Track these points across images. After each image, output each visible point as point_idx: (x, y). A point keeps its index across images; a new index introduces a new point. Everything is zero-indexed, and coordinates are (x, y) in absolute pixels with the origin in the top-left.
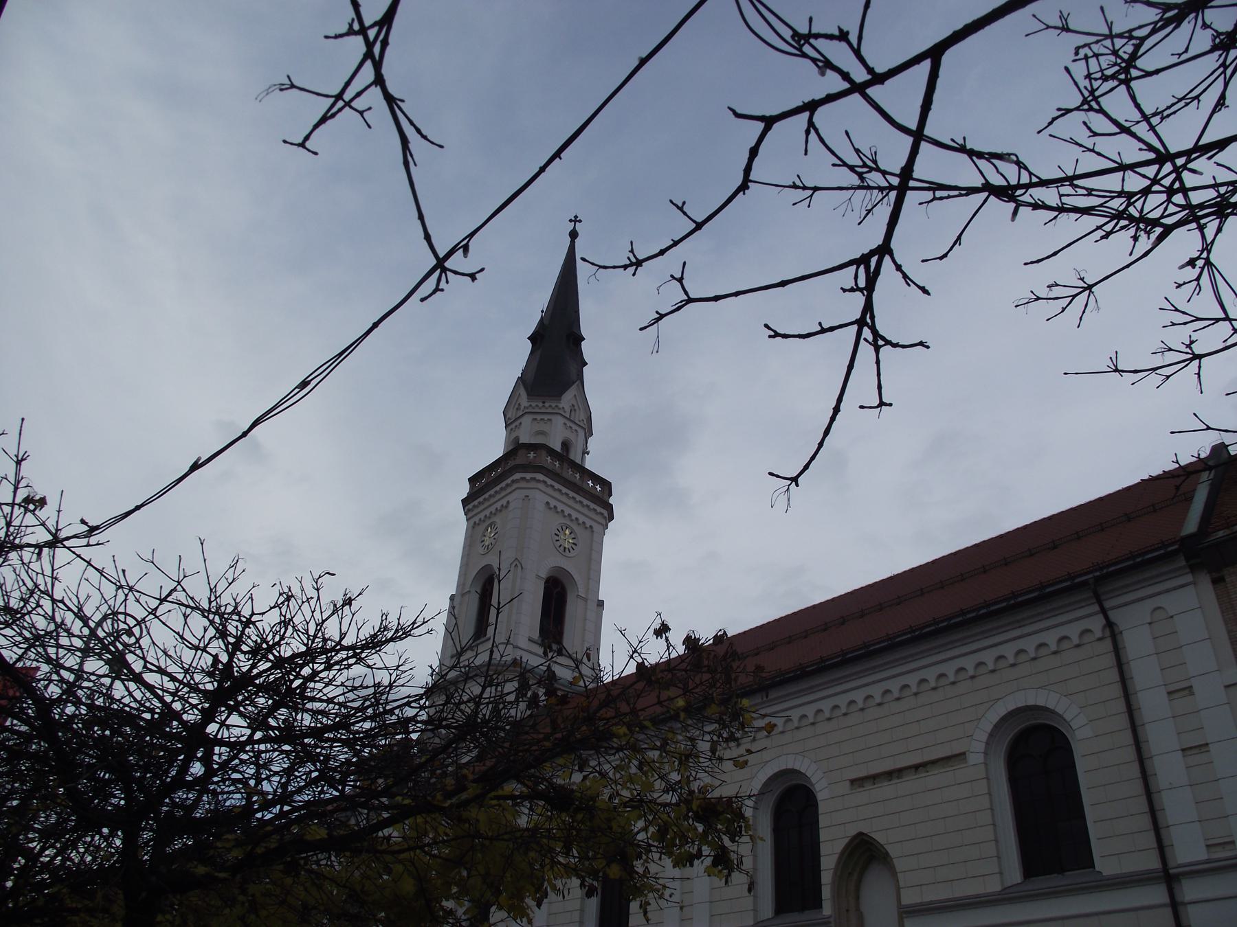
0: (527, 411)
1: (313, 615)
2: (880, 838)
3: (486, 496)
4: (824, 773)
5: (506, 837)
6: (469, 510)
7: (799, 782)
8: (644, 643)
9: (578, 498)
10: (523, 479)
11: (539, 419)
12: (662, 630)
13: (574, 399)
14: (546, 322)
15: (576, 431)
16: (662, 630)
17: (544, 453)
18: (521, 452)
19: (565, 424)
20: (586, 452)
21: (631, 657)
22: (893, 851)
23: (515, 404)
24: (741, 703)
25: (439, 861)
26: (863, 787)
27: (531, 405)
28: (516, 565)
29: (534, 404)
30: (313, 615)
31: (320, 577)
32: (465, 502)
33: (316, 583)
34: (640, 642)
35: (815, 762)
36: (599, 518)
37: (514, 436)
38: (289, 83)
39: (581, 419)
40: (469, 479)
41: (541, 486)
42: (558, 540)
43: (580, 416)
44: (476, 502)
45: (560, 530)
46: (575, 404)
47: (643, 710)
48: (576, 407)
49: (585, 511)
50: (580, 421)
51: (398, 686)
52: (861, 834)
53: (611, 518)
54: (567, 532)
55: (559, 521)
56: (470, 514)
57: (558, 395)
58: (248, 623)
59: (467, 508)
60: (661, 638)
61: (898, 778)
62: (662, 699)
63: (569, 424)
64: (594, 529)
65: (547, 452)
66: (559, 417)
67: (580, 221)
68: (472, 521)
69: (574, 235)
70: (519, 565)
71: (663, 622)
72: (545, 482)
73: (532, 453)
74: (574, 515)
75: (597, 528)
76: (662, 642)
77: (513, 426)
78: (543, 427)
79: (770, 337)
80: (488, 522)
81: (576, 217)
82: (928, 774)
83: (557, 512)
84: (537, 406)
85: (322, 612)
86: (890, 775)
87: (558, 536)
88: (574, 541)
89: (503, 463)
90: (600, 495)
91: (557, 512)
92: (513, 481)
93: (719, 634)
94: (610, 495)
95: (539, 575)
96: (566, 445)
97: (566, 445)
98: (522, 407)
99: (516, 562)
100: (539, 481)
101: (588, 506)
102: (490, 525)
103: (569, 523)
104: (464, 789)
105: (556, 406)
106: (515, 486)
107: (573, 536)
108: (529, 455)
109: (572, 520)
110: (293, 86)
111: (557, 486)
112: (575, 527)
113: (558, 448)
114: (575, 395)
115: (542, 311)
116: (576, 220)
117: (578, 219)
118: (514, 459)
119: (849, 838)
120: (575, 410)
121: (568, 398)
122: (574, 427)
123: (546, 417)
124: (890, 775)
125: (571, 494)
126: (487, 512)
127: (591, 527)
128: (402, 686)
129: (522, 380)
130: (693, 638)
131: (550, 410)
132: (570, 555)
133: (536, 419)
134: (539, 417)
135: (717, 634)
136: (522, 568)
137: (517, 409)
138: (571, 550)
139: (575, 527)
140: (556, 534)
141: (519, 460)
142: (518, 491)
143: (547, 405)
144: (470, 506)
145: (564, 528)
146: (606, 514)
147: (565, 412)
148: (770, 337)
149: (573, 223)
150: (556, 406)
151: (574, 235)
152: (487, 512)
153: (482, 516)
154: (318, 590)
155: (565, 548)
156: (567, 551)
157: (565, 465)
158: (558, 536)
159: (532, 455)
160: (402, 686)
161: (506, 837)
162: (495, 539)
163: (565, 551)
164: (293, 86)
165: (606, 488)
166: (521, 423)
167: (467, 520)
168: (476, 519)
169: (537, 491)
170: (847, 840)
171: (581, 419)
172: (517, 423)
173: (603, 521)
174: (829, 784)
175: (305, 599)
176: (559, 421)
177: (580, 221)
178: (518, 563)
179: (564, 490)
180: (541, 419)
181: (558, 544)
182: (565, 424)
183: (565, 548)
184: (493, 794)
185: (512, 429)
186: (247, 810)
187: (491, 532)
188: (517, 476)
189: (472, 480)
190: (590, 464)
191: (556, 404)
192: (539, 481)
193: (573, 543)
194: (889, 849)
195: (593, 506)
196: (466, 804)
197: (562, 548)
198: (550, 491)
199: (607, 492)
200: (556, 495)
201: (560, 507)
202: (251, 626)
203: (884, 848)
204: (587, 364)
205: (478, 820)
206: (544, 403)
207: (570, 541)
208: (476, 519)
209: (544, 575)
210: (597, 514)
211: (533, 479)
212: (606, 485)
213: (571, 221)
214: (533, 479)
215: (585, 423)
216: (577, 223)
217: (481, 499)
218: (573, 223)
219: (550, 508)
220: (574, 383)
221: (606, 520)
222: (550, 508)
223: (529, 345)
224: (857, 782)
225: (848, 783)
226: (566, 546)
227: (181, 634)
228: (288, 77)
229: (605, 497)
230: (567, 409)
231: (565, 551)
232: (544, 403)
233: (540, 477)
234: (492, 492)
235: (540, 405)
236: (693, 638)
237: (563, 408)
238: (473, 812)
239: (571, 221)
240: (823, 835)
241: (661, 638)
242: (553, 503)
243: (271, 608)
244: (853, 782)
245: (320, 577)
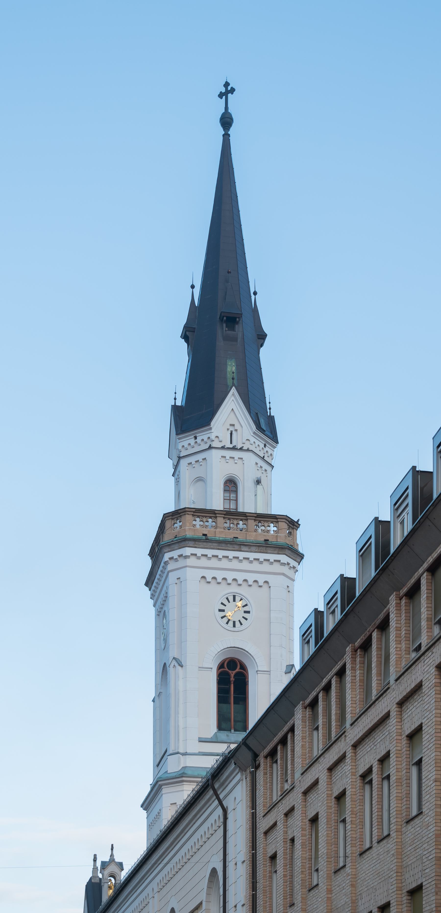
9: (241, 555)
13: (232, 413)
28: (174, 666)
36: (276, 568)
39: (244, 441)
41: (191, 561)
48: (237, 426)
74: (240, 577)
81: (227, 84)
83: (219, 583)
99: (174, 662)
103: (234, 589)
112: (243, 591)
114: (232, 409)
120: (236, 430)
122: (236, 454)
123: (200, 457)
125: (231, 554)
138: (243, 621)
139: (243, 591)
143: (199, 440)
146: (284, 558)
150: (209, 438)
155: (234, 622)
163: (234, 626)
165: (283, 525)
171: (244, 441)
177: (233, 90)
191: (208, 436)
198: (204, 562)
201: (219, 575)
215: (252, 440)
216: (230, 95)
231: (234, 626)
233: (188, 551)
235: (192, 441)
237: (217, 437)
242: (209, 576)
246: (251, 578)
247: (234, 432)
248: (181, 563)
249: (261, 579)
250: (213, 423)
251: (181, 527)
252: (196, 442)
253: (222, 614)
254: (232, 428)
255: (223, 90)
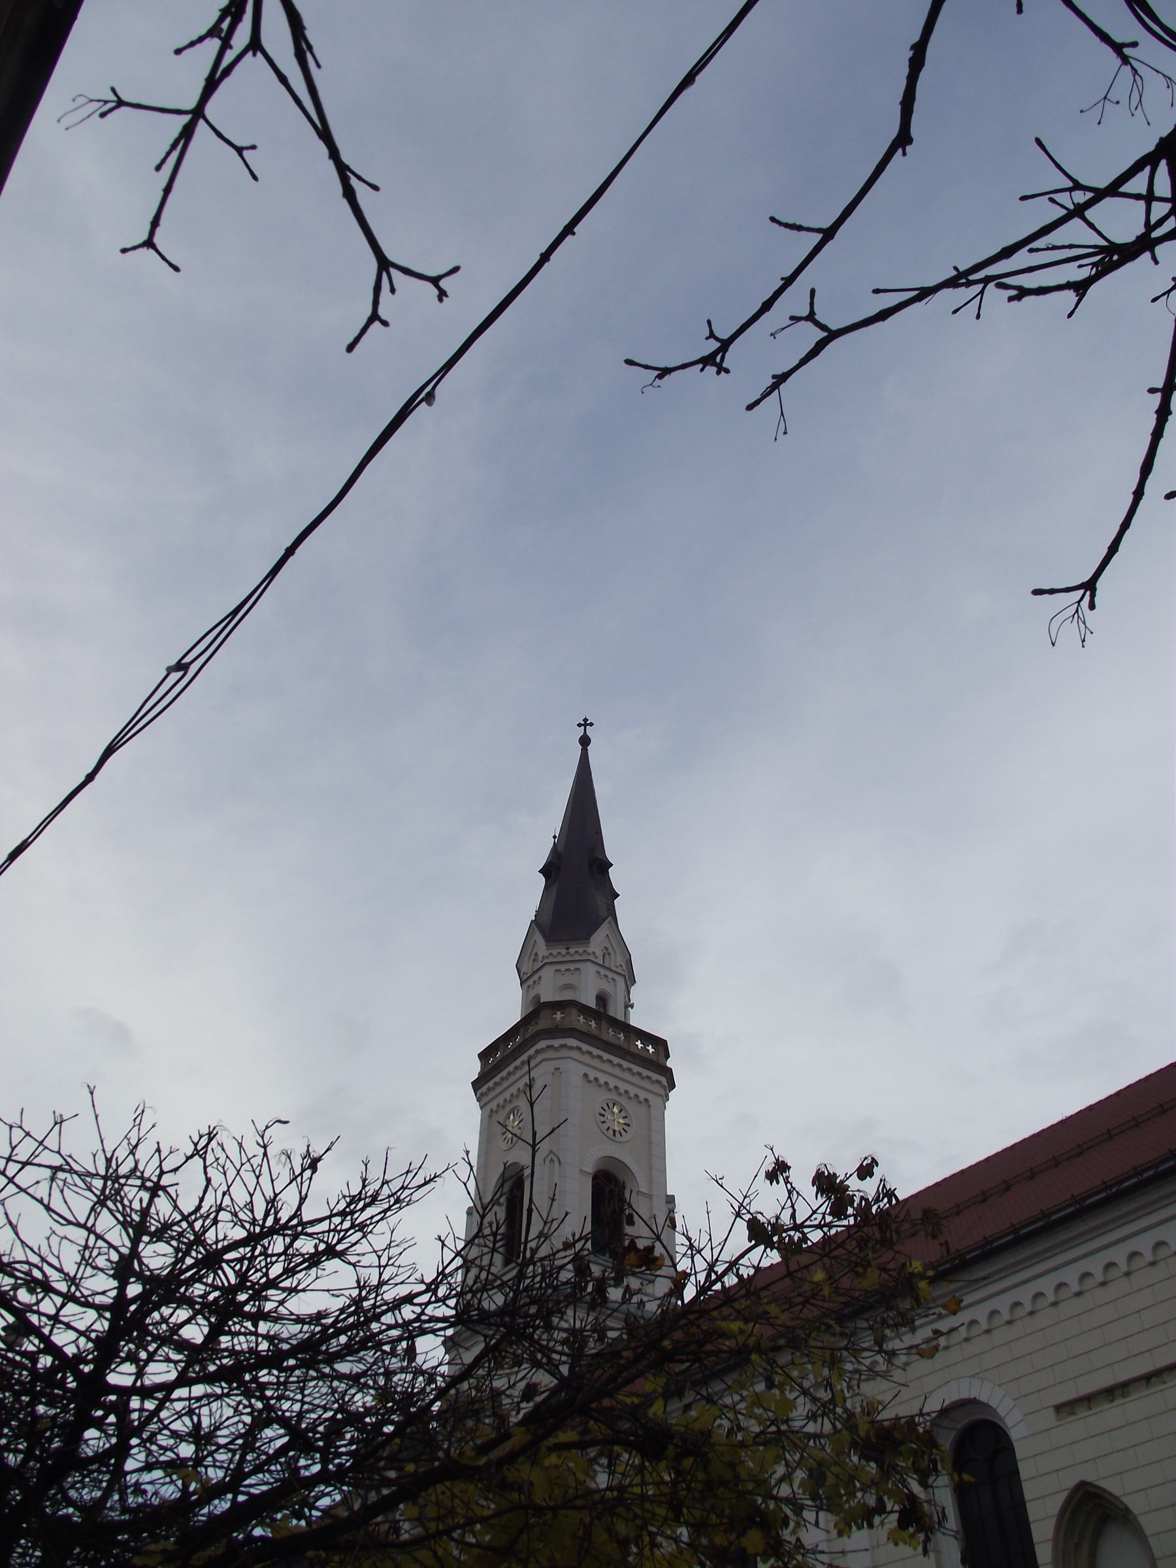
0: (546, 961)
1: (258, 1183)
2: (1113, 1486)
3: (504, 1073)
4: (1015, 1400)
5: (578, 1503)
6: (482, 1095)
7: (981, 1417)
8: (752, 1197)
9: (625, 1064)
10: (550, 1047)
11: (563, 969)
12: (778, 1171)
14: (560, 849)
15: (614, 979)
16: (778, 1171)
17: (574, 1012)
18: (545, 1014)
19: (598, 972)
20: (629, 1005)
21: (738, 1215)
22: (1135, 1504)
23: (531, 952)
24: (911, 1265)
25: (476, 1551)
26: (1075, 1414)
27: (551, 954)
28: (552, 1160)
29: (555, 952)
30: (258, 1183)
31: (267, 1127)
32: (476, 1085)
33: (262, 1137)
34: (745, 1197)
35: (999, 1386)
37: (533, 993)
38: (115, 99)
39: (618, 965)
40: (479, 1055)
42: (605, 1122)
43: (617, 960)
44: (491, 1084)
45: (606, 1108)
46: (608, 946)
47: (765, 1288)
48: (610, 950)
49: (636, 1080)
50: (617, 967)
51: (397, 1284)
52: (1083, 1484)
53: (672, 1085)
54: (616, 1110)
55: (603, 1096)
56: (485, 1100)
57: (586, 937)
58: (156, 1190)
59: (479, 1092)
60: (778, 1183)
61: (1124, 1396)
62: (792, 1269)
63: (603, 971)
64: (651, 1102)
65: (579, 1011)
66: (589, 964)
67: (591, 724)
68: (488, 1108)
69: (585, 741)
70: (554, 1158)
71: (777, 1160)
72: (579, 1049)
73: (559, 1013)
74: (623, 1087)
75: (653, 1100)
76: (780, 1189)
77: (530, 982)
78: (569, 979)
79: (1011, 299)
80: (509, 1107)
81: (586, 720)
82: (1164, 1386)
83: (600, 1086)
84: (559, 953)
85: (272, 1181)
86: (1112, 1393)
87: (604, 1116)
88: (626, 1121)
89: (522, 1030)
90: (654, 1058)
91: (600, 1086)
92: (537, 1052)
93: (864, 1164)
94: (667, 1056)
95: (584, 1169)
96: (602, 999)
97: (602, 999)
98: (540, 958)
99: (552, 1156)
100: (571, 1048)
101: (639, 1074)
102: (512, 1111)
104: (507, 1436)
105: (585, 951)
106: (540, 1057)
107: (623, 1115)
108: (555, 1016)
109: (620, 1094)
110: (120, 103)
111: (596, 1052)
113: (592, 1003)
115: (555, 837)
116: (586, 724)
117: (588, 722)
118: (536, 1023)
119: (1069, 1491)
120: (609, 954)
121: (598, 940)
122: (610, 975)
123: (572, 967)
124: (1112, 1393)
125: (616, 1060)
126: (507, 1095)
127: (646, 1100)
128: (402, 1283)
129: (536, 924)
130: (826, 1174)
131: (577, 957)
132: (623, 1139)
133: (559, 970)
134: (563, 967)
135: (862, 1165)
136: (560, 1163)
137: (534, 960)
139: (623, 1101)
140: (601, 1114)
141: (543, 1023)
142: (544, 1063)
143: (572, 951)
144: (484, 1089)
145: (611, 1105)
146: (664, 1081)
147: (596, 957)
148: (1011, 299)
149: (583, 727)
150: (585, 951)
151: (585, 741)
152: (507, 1095)
153: (500, 1100)
154: (265, 1147)
155: (614, 1131)
156: (617, 1134)
157: (604, 1024)
158: (604, 1116)
159: (559, 1016)
160: (402, 1283)
161: (578, 1503)
162: (520, 1128)
163: (614, 1135)
164: (120, 103)
165: (661, 1048)
166: (540, 978)
167: (481, 1108)
168: (493, 1105)
169: (570, 1060)
170: (1064, 1496)
171: (618, 965)
172: (535, 978)
173: (662, 1092)
174: (1025, 1416)
175: (245, 1159)
176: (590, 970)
177: (591, 724)
178: (554, 1158)
179: (606, 1056)
180: (566, 970)
181: (605, 1126)
182: (598, 972)
183: (614, 1131)
184: (552, 1441)
185: (529, 986)
186: (184, 1506)
187: (514, 1121)
188: (542, 1044)
189: (483, 1056)
190: (636, 1020)
192: (571, 1048)
193: (625, 1124)
194: (1127, 1500)
195: (645, 1072)
196: (511, 1458)
197: (611, 1132)
198: (586, 1059)
199: (662, 1053)
200: (596, 1063)
201: (603, 1078)
202: (160, 1193)
203: (1122, 1502)
204: (619, 895)
205: (531, 1484)
206: (568, 949)
207: (621, 1121)
208: (493, 1105)
209: (590, 1168)
210: (653, 1082)
211: (563, 1046)
212: (661, 1045)
213: (580, 725)
214: (563, 1046)
215: (624, 968)
216: (588, 727)
217: (497, 1079)
218: (583, 727)
219: (590, 1082)
220: (604, 920)
221: (665, 1090)
222: (590, 1082)
223: (541, 881)
224: (1065, 1409)
225: (1052, 1410)
226: (617, 1128)
227: (46, 1202)
228: (113, 90)
229: (661, 1060)
230: (599, 954)
231: (614, 1135)
232: (568, 949)
233: (572, 1042)
234: (511, 1068)
235: (564, 951)
236: (826, 1174)
237: (594, 953)
238: (523, 1471)
239: (580, 725)
240: (1030, 1491)
241: (778, 1183)
242: (592, 1074)
243: (188, 1158)
244: (1059, 1408)
245: (267, 1127)
246: (633, 1091)
247: (607, 955)
248: (564, 1053)
249: (642, 1095)
250: (592, 938)
251: (563, 1018)
252: (568, 953)
253: (603, 1119)
254: (605, 951)
255: (583, 723)
